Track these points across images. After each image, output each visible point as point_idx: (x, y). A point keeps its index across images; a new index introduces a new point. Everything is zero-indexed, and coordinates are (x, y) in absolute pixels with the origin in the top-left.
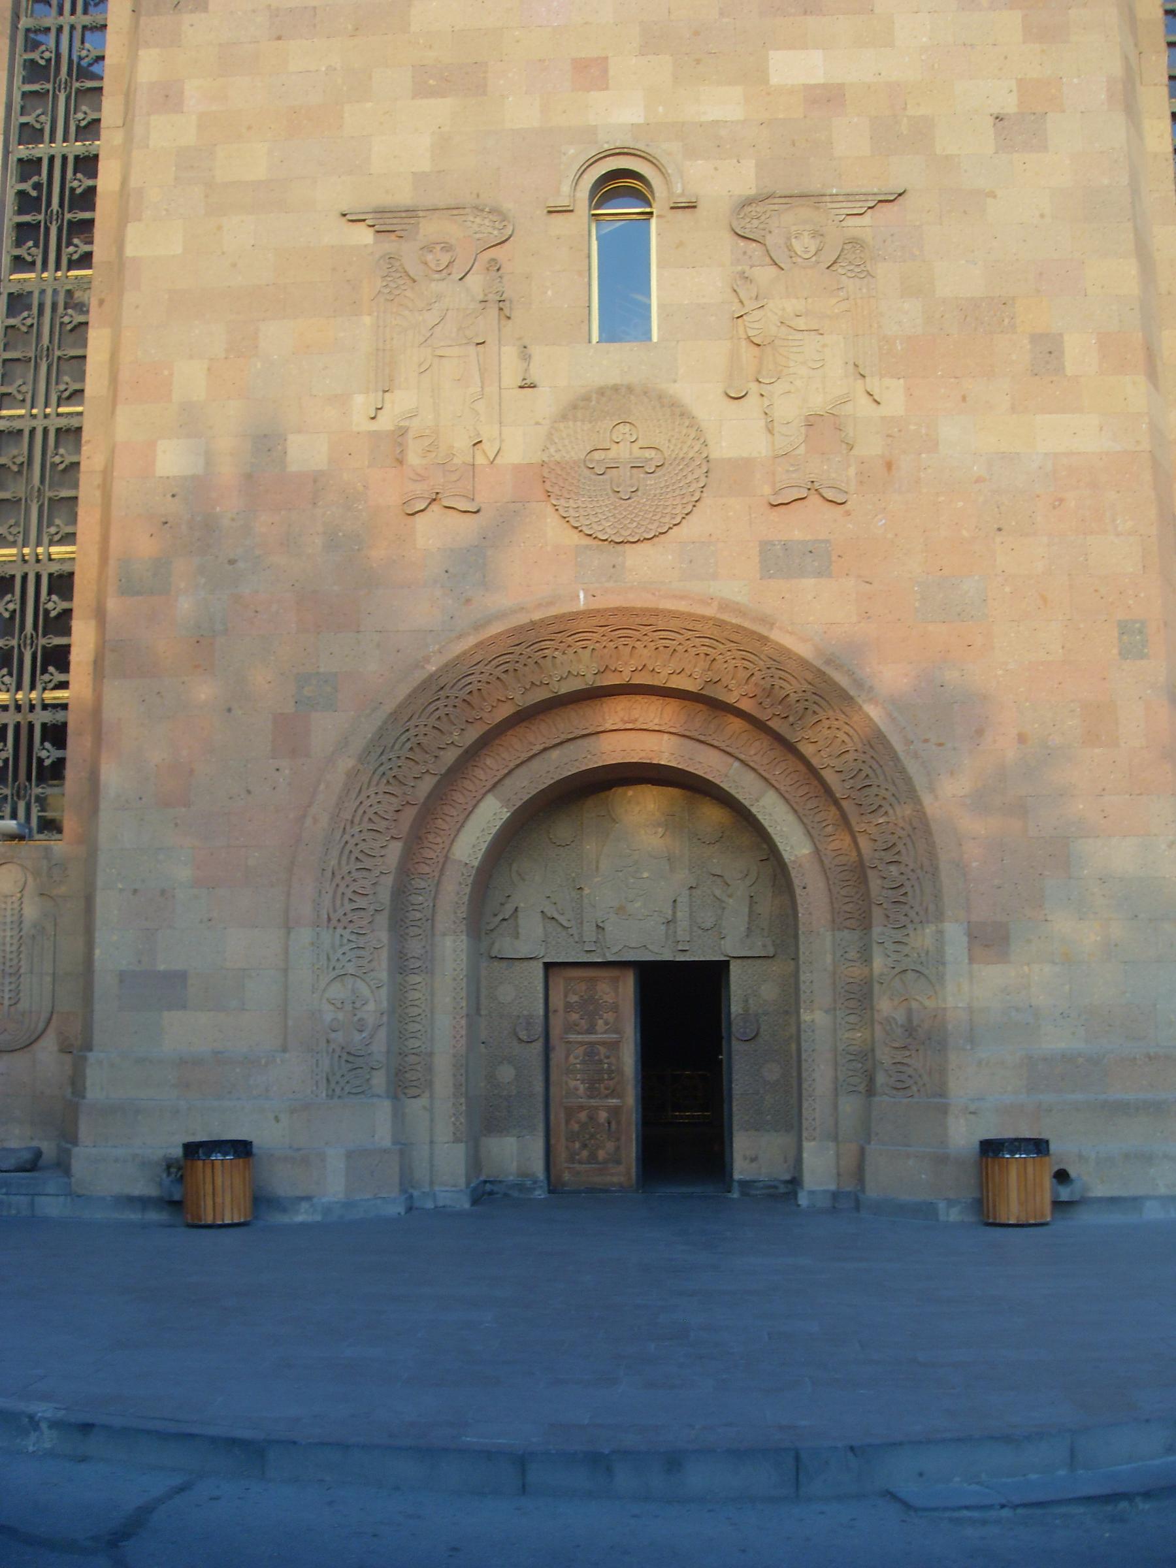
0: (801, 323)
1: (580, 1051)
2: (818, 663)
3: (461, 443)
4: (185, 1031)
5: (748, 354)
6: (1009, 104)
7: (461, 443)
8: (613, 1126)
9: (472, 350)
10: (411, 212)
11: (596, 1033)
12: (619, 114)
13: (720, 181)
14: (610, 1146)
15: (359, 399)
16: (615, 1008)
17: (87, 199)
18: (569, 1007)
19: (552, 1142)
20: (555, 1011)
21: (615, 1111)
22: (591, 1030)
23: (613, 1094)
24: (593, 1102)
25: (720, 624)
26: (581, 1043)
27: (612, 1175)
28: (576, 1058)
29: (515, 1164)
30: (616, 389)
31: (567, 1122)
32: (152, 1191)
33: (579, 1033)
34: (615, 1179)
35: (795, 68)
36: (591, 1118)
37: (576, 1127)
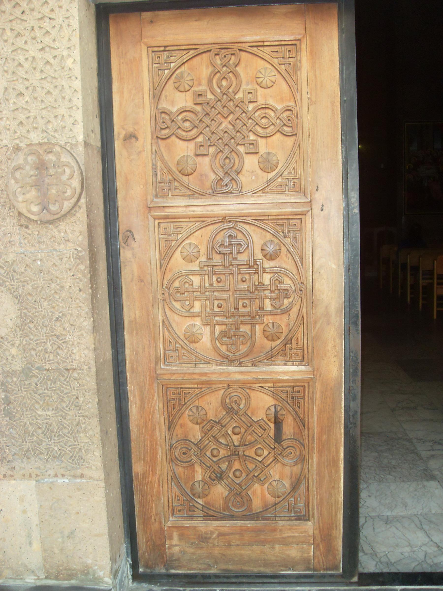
1: (200, 239)
8: (288, 429)
11: (240, 193)
14: (281, 474)
16: (290, 124)
18: (165, 127)
19: (138, 468)
20: (131, 137)
21: (294, 395)
22: (227, 182)
24: (235, 372)
26: (203, 221)
27: (285, 542)
28: (188, 259)
29: (36, 546)
31: (171, 425)
33: (195, 194)
34: (294, 552)
36: (230, 410)
37: (196, 433)
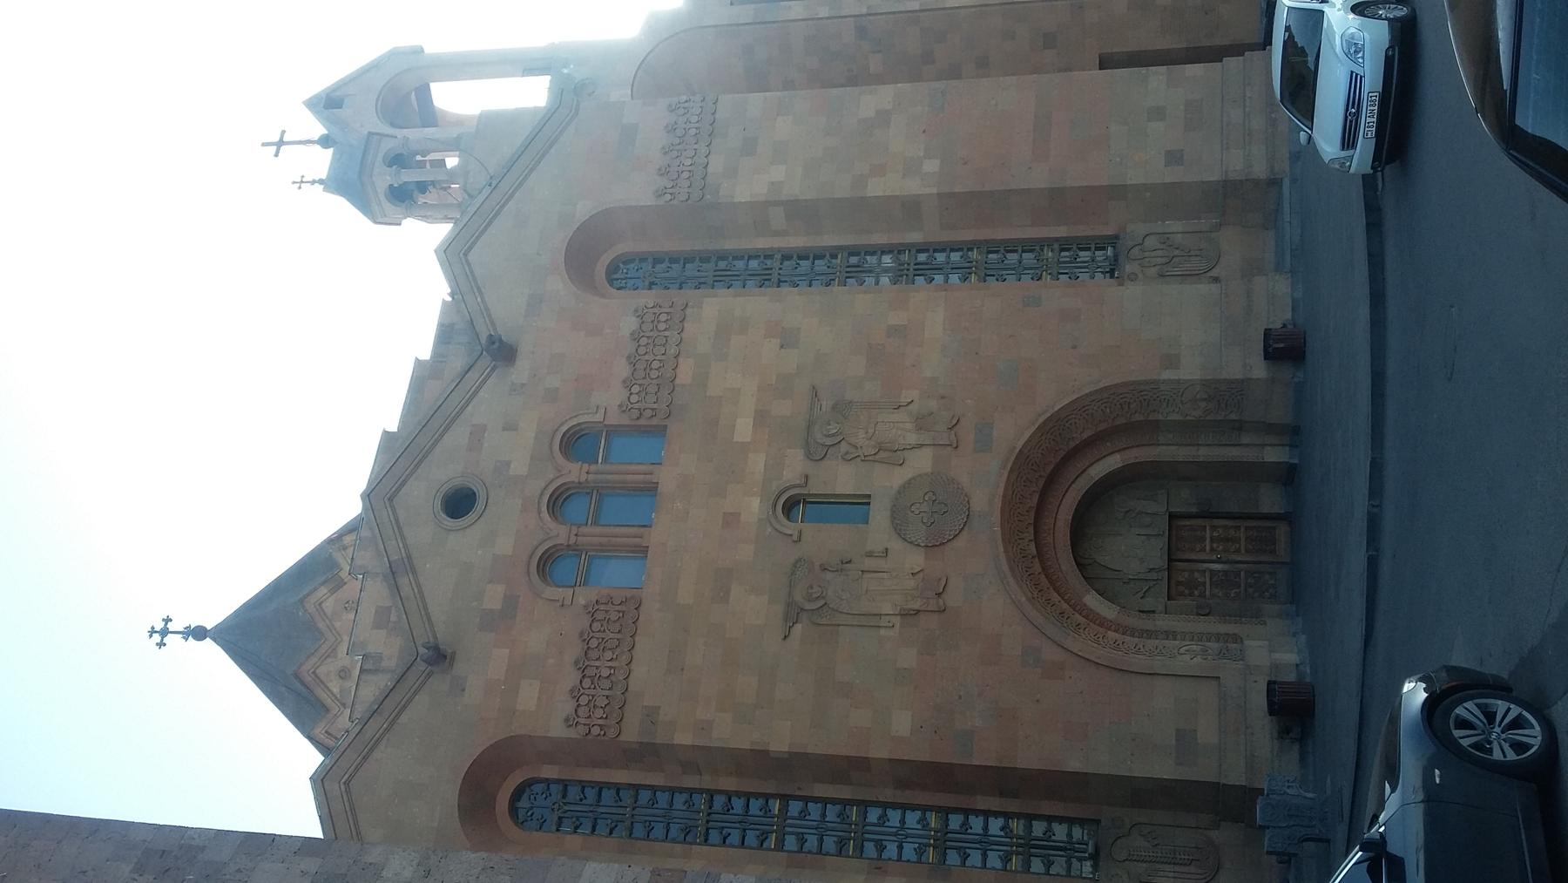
0: (871, 431)
2: (1033, 429)
3: (911, 583)
4: (1207, 732)
5: (882, 455)
6: (776, 342)
7: (911, 583)
9: (867, 575)
10: (789, 605)
12: (754, 507)
15: (882, 632)
23: (1238, 574)
25: (1011, 470)
30: (893, 512)
32: (1296, 747)
35: (744, 429)
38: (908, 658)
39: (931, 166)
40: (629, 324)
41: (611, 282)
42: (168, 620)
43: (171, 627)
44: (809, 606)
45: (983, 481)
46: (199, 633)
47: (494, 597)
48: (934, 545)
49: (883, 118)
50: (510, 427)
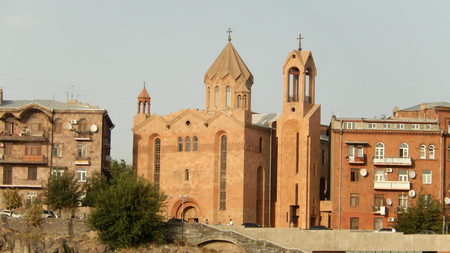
6: (208, 164)
12: (187, 165)
13: (192, 170)
17: (159, 168)
35: (197, 162)
38: (170, 188)
39: (231, 183)
40: (211, 143)
41: (224, 136)
42: (232, 32)
43: (231, 33)
44: (176, 174)
45: (191, 195)
46: (230, 40)
47: (177, 132)
48: (183, 190)
49: (239, 175)
50: (198, 128)
